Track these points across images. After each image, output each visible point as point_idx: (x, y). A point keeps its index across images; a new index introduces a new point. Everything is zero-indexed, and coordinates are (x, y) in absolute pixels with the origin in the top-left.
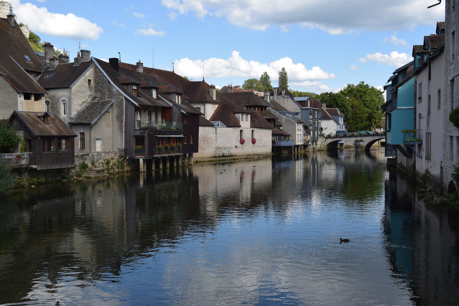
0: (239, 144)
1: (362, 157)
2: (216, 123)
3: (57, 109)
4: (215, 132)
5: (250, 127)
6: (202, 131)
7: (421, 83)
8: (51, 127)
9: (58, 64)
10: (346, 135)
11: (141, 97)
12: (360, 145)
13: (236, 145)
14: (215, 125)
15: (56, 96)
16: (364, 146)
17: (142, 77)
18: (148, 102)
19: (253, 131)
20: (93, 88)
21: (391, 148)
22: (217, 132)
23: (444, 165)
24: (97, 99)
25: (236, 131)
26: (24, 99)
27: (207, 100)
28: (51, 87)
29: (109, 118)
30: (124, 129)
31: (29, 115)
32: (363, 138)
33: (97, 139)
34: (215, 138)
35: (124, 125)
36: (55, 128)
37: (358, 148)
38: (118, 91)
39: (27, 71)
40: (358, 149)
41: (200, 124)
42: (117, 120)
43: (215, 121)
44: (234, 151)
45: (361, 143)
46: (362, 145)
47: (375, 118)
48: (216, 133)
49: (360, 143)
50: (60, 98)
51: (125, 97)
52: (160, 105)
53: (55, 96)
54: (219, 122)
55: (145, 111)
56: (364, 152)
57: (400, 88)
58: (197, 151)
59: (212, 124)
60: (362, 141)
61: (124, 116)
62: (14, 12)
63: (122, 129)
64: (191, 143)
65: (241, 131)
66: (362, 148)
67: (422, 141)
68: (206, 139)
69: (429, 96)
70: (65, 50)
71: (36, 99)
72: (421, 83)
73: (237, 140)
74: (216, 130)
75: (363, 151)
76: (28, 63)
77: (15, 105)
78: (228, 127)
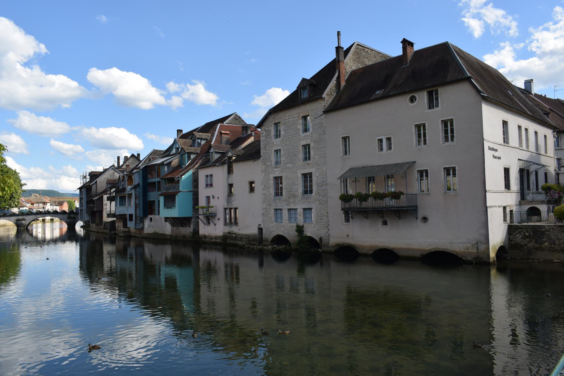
1: (24, 236)
7: (211, 175)
10: (6, 215)
12: (22, 224)
16: (26, 225)
21: (139, 222)
23: (264, 227)
32: (25, 217)
37: (21, 227)
40: (20, 228)
45: (24, 222)
46: (24, 224)
47: (14, 198)
49: (23, 221)
56: (26, 230)
57: (183, 177)
60: (24, 220)
66: (24, 227)
67: (216, 214)
69: (231, 186)
72: (211, 175)
75: (25, 229)
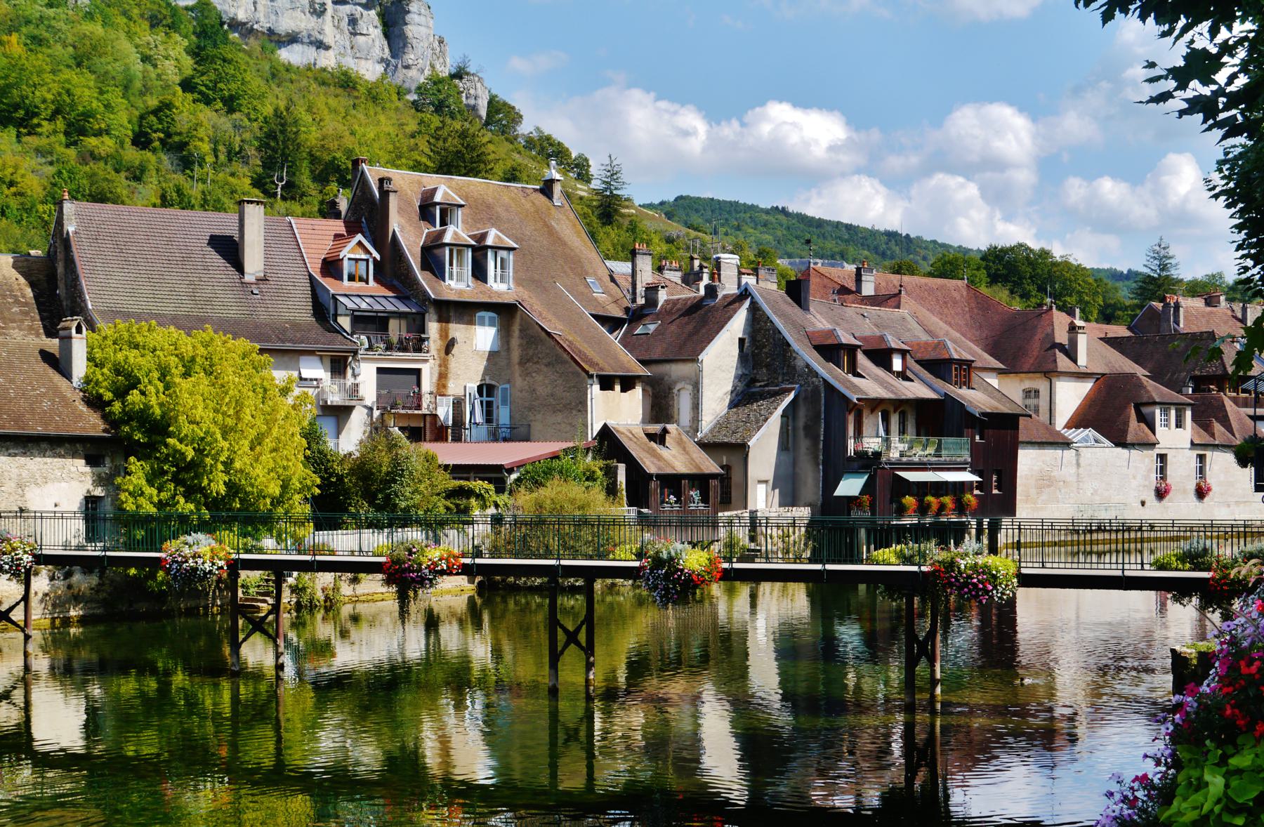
0: (1150, 497)
2: (1076, 435)
3: (667, 409)
4: (1074, 462)
5: (1189, 446)
6: (1028, 461)
8: (674, 456)
9: (665, 297)
11: (864, 377)
13: (1143, 498)
14: (1075, 440)
15: (666, 378)
17: (867, 320)
18: (879, 390)
19: (1202, 458)
20: (750, 358)
22: (1082, 461)
24: (758, 384)
25: (1143, 461)
26: (601, 389)
27: (1056, 367)
28: (655, 357)
29: (788, 430)
30: (821, 457)
31: (631, 433)
33: (760, 482)
34: (1074, 479)
35: (821, 446)
36: (682, 458)
38: (808, 366)
39: (596, 317)
41: (1020, 439)
42: (806, 436)
43: (1077, 427)
44: (1134, 514)
48: (1078, 465)
50: (675, 382)
51: (824, 379)
52: (910, 396)
53: (663, 379)
54: (1090, 433)
55: (872, 411)
58: (1011, 511)
59: (1066, 438)
61: (823, 425)
62: (494, 92)
63: (816, 457)
64: (995, 492)
65: (1162, 458)
68: (1046, 481)
70: (615, 163)
71: (624, 390)
73: (1147, 483)
74: (1078, 455)
76: (596, 299)
77: (581, 403)
78: (1117, 445)
